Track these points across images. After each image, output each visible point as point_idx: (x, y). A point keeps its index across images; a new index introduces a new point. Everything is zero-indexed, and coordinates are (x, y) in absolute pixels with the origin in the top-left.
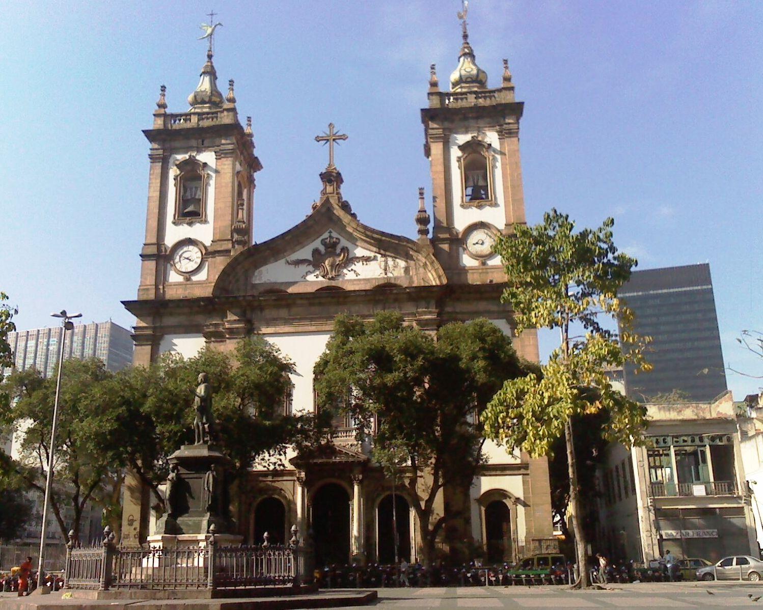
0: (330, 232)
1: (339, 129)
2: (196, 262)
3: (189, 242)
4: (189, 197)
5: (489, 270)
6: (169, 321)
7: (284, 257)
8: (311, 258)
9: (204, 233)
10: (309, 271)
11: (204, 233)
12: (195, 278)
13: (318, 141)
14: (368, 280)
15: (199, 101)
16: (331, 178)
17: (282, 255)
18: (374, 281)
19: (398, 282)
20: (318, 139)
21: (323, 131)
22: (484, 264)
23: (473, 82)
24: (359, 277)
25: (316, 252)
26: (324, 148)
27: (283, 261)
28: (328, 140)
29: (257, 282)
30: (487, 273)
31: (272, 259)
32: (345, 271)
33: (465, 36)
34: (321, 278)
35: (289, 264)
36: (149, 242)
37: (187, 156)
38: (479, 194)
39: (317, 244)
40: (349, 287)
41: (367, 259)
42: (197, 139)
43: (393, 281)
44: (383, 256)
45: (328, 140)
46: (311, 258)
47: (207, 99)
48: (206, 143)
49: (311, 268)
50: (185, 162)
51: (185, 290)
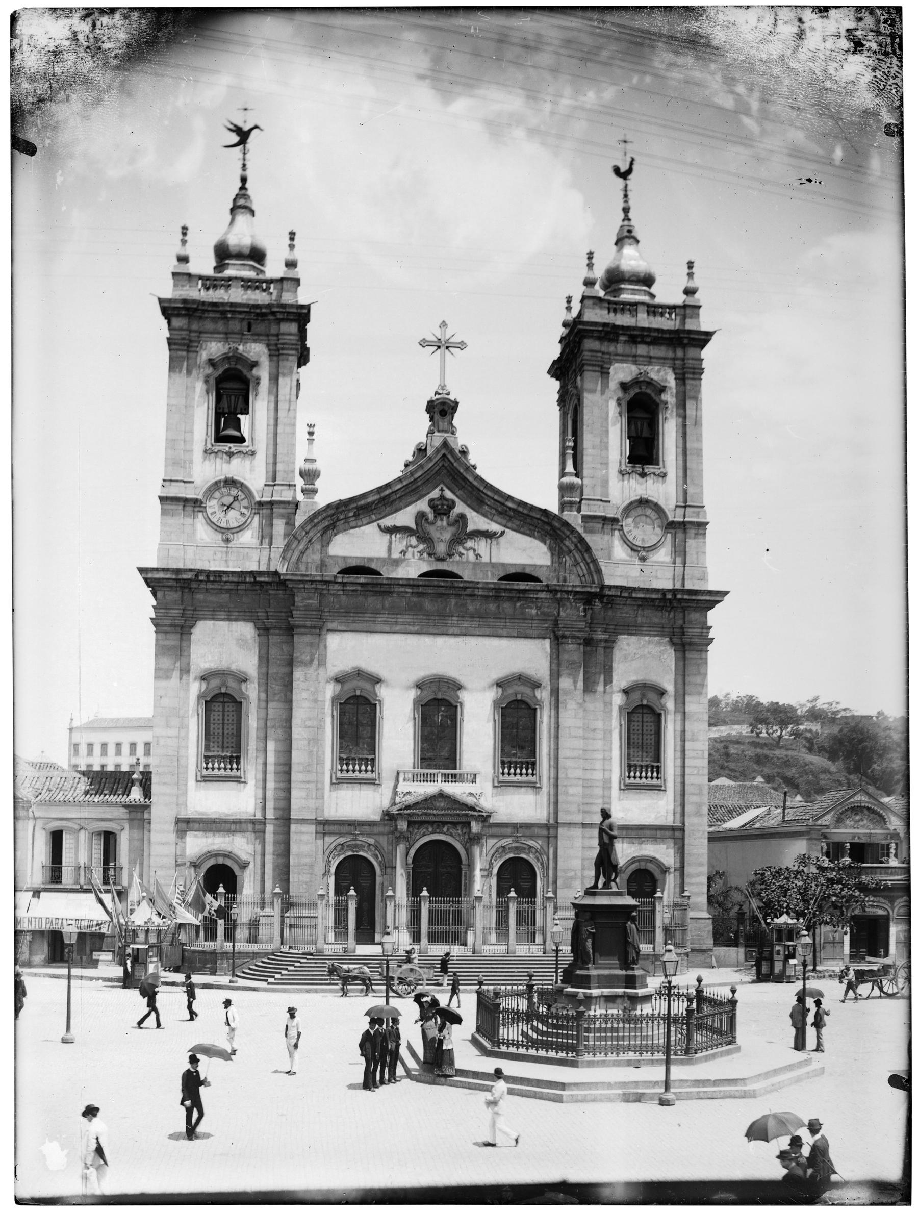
1: (455, 332)
8: (413, 526)
20: (424, 343)
25: (421, 517)
26: (431, 359)
27: (375, 524)
39: (422, 505)
40: (467, 575)
45: (439, 347)
46: (413, 526)
49: (413, 541)
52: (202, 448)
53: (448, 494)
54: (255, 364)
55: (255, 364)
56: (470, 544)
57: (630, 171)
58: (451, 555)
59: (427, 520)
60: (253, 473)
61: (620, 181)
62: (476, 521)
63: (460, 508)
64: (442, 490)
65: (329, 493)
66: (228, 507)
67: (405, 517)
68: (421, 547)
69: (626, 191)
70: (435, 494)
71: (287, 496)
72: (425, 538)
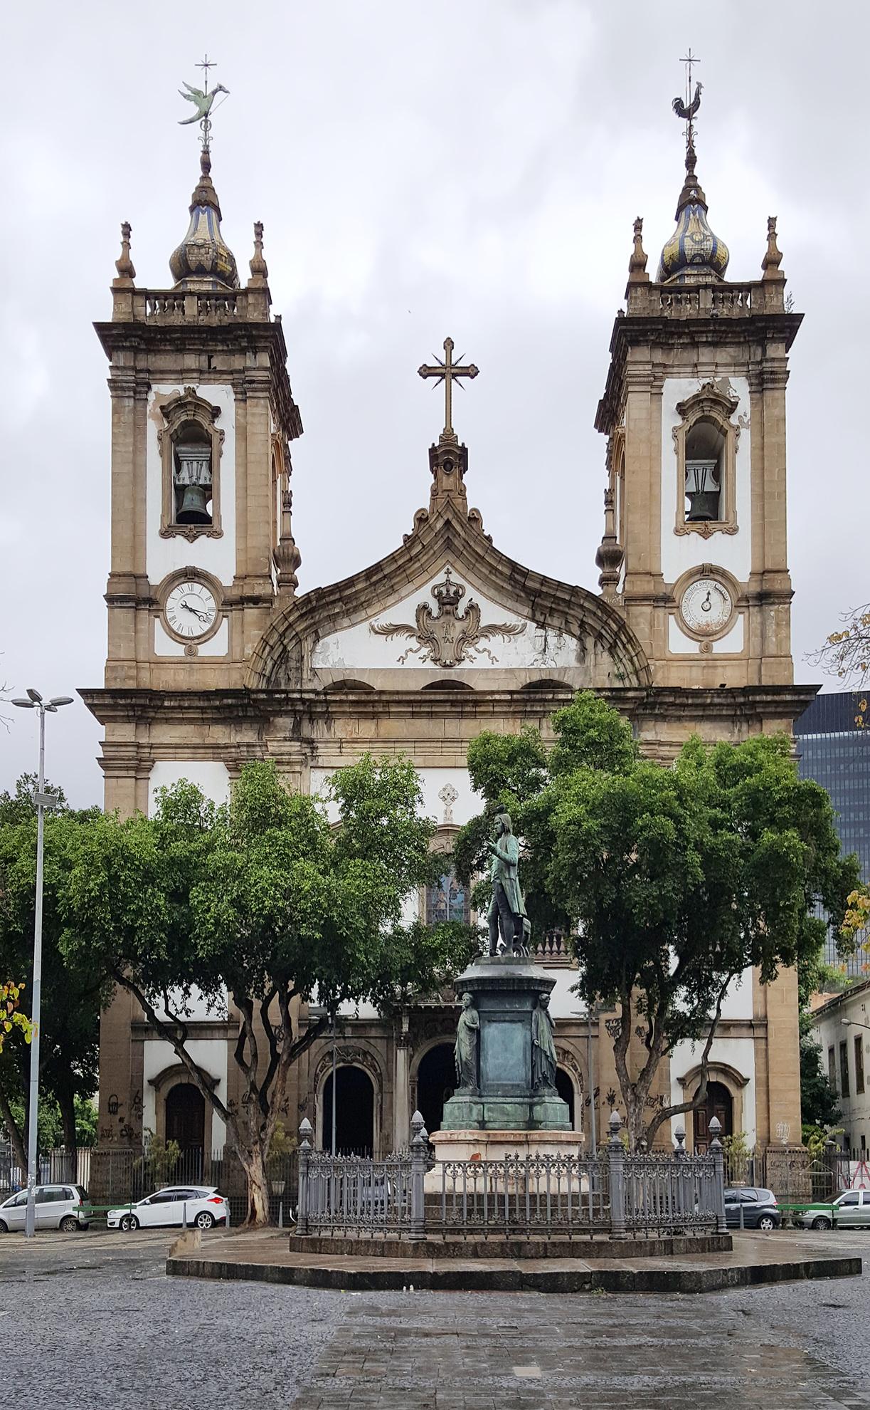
0: (448, 573)
1: (464, 356)
3: (191, 575)
4: (187, 482)
5: (718, 663)
6: (166, 734)
7: (369, 617)
8: (414, 625)
9: (218, 555)
10: (411, 650)
11: (218, 555)
14: (510, 671)
15: (193, 268)
16: (449, 458)
18: (523, 674)
19: (566, 680)
22: (707, 649)
23: (704, 264)
24: (496, 665)
25: (423, 609)
27: (366, 625)
30: (715, 667)
31: (346, 622)
32: (471, 651)
33: (691, 161)
34: (429, 664)
35: (377, 633)
36: (119, 570)
38: (706, 511)
39: (424, 595)
40: (479, 684)
41: (507, 630)
43: (556, 677)
44: (542, 625)
46: (414, 625)
47: (208, 265)
49: (413, 643)
53: (455, 578)
56: (483, 643)
57: (696, 104)
58: (460, 660)
59: (430, 613)
61: (684, 121)
62: (492, 613)
63: (472, 594)
64: (448, 573)
65: (309, 579)
67: (403, 611)
68: (425, 651)
69: (690, 135)
70: (440, 578)
71: (259, 590)
72: (426, 638)
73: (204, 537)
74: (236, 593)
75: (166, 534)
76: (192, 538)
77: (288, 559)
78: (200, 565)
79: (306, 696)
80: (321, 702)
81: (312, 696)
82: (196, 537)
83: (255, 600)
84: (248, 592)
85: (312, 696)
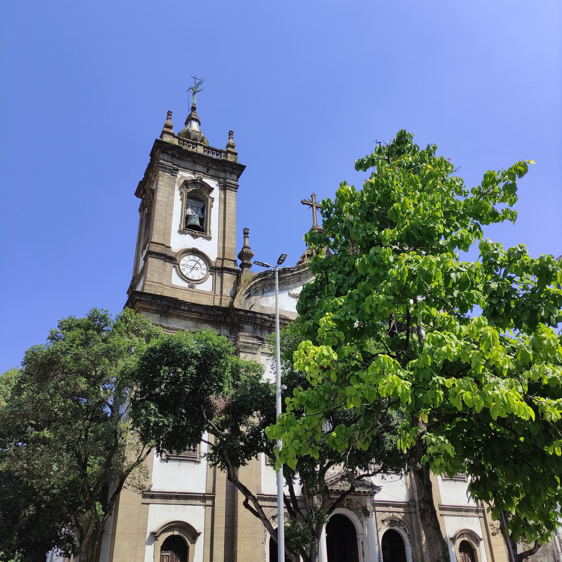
2: (202, 273)
3: (194, 252)
11: (211, 248)
12: (198, 287)
13: (304, 204)
15: (192, 138)
17: (286, 286)
21: (308, 198)
28: (312, 206)
29: (264, 305)
35: (291, 296)
37: (193, 177)
42: (203, 166)
48: (211, 172)
50: (194, 182)
51: (192, 296)
52: (178, 229)
54: (211, 189)
55: (211, 189)
60: (211, 248)
66: (194, 267)
71: (231, 265)
73: (201, 238)
74: (219, 265)
75: (180, 232)
76: (195, 237)
77: (244, 255)
78: (200, 249)
79: (265, 317)
80: (269, 321)
81: (268, 318)
82: (197, 237)
83: (229, 270)
84: (225, 265)
85: (268, 318)
